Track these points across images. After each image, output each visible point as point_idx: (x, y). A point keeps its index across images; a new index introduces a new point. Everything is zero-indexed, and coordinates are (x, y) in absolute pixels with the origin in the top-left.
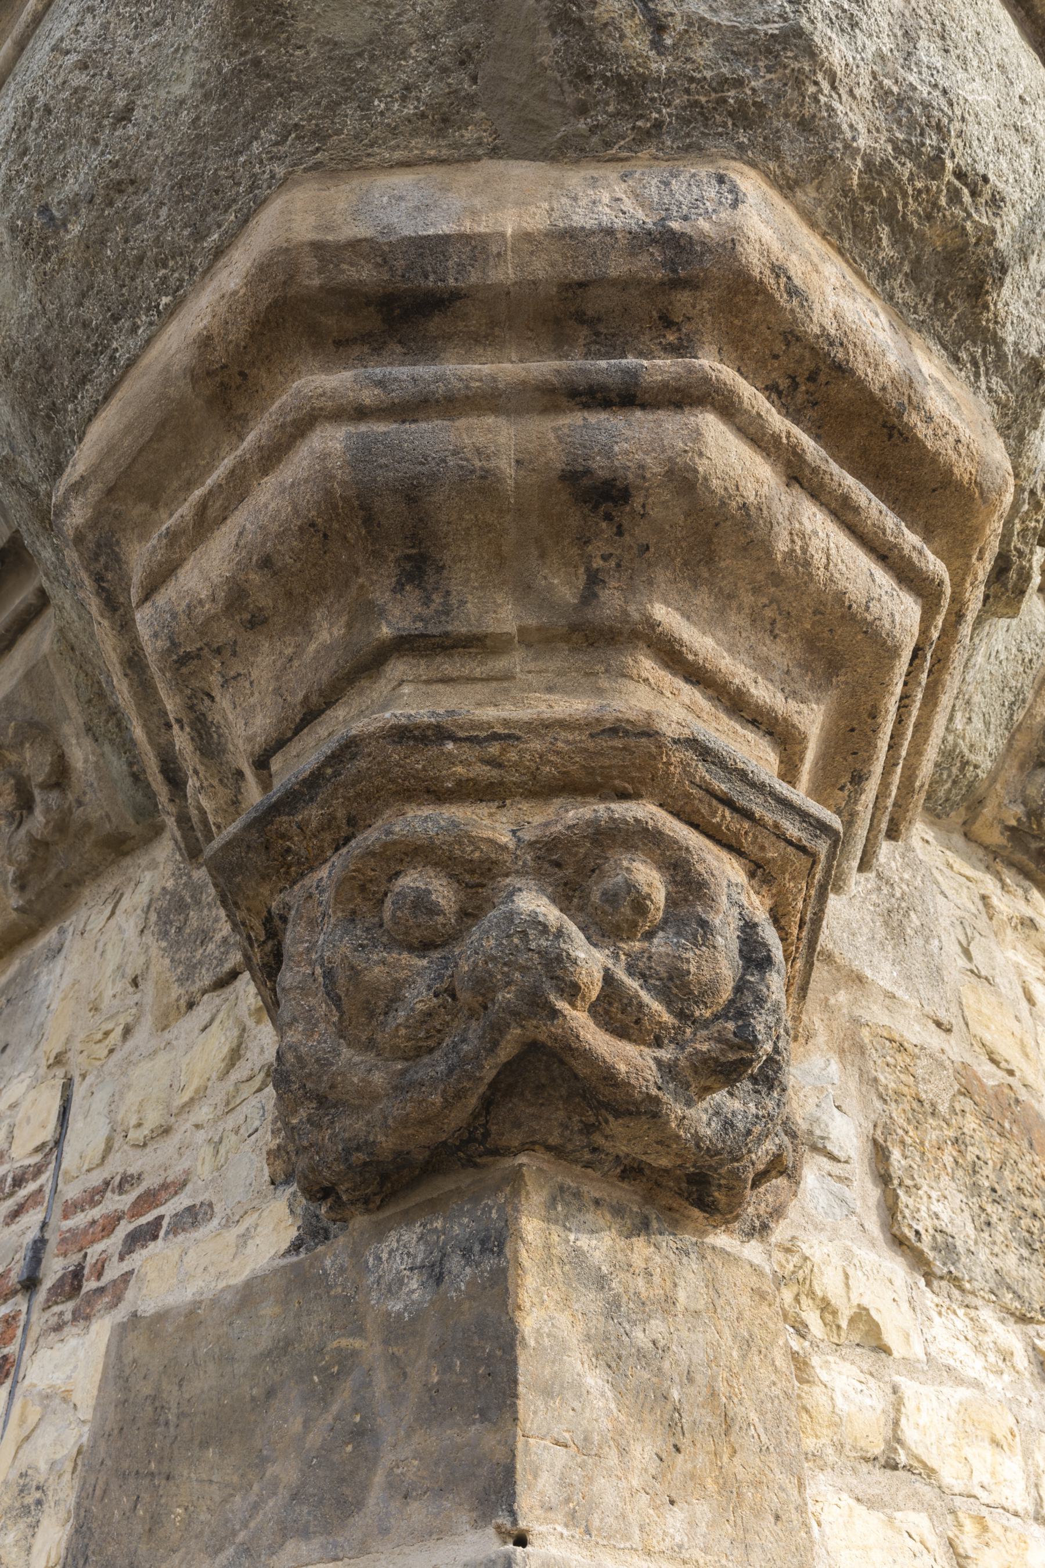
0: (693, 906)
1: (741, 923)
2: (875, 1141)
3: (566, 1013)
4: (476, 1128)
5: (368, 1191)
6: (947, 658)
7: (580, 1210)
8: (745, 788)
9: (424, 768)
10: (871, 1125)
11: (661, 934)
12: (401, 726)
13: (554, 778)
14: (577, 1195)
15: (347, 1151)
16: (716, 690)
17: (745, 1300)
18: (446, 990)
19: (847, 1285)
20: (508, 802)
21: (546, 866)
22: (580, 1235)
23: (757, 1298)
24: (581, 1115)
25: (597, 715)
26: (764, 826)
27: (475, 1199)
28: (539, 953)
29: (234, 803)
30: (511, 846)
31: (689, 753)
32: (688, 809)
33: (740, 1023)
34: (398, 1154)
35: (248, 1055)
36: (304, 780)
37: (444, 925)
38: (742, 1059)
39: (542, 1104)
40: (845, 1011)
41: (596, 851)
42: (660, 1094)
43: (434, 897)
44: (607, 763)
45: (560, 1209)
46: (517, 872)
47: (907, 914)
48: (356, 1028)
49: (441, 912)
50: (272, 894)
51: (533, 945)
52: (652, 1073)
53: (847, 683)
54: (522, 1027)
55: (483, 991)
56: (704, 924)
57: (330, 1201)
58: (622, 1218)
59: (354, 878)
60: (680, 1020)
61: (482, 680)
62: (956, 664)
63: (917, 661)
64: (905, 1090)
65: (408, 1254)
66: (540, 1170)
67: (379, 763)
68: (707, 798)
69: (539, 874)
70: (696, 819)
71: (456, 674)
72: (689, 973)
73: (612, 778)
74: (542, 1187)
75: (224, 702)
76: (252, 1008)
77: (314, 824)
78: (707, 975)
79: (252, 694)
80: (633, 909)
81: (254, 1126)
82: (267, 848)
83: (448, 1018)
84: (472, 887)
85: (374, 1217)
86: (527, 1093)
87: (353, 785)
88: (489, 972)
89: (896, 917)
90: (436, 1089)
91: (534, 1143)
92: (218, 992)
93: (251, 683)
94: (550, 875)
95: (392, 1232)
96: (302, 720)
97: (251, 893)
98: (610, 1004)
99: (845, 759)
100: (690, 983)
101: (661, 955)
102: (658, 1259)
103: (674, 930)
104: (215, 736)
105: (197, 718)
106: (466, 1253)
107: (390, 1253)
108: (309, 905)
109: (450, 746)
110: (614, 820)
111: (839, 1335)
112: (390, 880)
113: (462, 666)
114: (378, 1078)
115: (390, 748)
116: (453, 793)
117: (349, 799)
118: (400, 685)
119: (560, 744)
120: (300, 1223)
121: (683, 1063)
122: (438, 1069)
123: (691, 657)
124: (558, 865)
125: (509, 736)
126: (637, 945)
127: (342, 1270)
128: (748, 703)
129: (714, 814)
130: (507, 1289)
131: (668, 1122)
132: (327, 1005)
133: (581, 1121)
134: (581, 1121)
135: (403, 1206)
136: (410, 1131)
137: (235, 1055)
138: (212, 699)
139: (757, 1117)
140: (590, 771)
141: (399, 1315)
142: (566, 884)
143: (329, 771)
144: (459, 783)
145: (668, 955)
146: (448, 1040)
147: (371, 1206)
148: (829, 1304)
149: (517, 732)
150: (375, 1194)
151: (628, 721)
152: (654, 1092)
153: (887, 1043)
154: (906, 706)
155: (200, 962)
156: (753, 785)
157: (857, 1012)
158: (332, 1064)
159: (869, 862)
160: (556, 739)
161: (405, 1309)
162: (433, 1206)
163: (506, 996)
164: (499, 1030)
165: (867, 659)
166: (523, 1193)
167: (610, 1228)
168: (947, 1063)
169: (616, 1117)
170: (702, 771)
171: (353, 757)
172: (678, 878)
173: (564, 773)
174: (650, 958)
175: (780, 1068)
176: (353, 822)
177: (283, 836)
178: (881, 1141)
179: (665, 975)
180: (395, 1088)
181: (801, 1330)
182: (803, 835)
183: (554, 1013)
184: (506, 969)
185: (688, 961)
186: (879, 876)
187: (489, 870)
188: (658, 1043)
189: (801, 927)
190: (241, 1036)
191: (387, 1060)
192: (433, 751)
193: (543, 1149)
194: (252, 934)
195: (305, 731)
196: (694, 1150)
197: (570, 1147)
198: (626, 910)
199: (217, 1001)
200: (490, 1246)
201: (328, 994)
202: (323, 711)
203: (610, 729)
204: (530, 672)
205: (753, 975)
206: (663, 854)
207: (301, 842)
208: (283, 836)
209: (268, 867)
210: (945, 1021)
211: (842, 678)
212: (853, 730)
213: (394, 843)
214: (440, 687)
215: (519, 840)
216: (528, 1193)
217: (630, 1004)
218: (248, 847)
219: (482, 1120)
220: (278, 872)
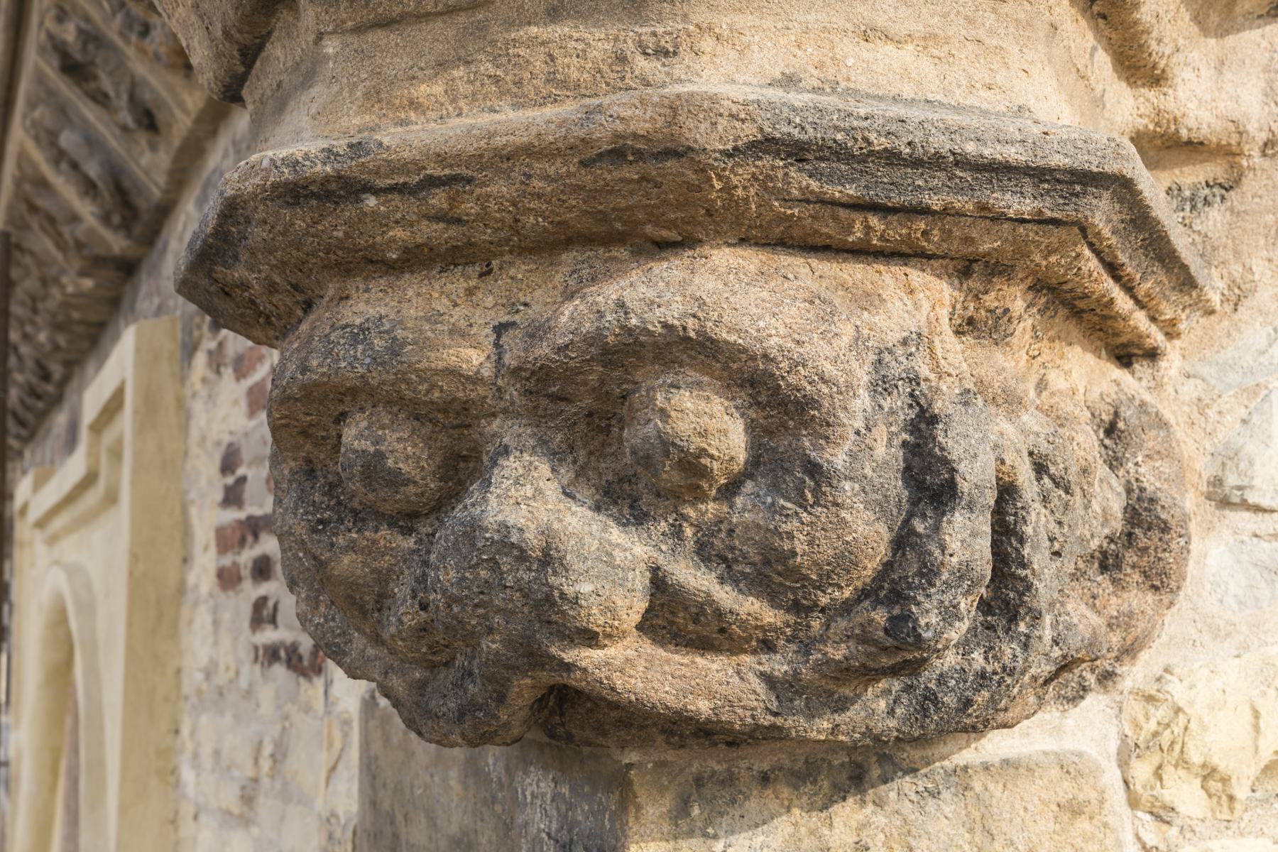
0: (797, 437)
1: (912, 414)
3: (584, 664)
7: (733, 801)
8: (897, 174)
12: (286, 184)
13: (545, 230)
14: (729, 780)
17: (1046, 825)
19: (1256, 728)
21: (544, 402)
22: (732, 839)
23: (1066, 817)
25: (582, 134)
26: (960, 214)
28: (521, 590)
30: (487, 372)
31: (767, 161)
32: (796, 232)
33: (896, 611)
38: (905, 661)
42: (779, 721)
44: (623, 203)
46: (505, 411)
49: (408, 482)
56: (813, 469)
58: (815, 782)
60: (798, 614)
66: (661, 765)
67: (283, 234)
68: (828, 210)
69: (536, 416)
70: (819, 241)
72: (794, 554)
74: (662, 790)
78: (827, 551)
80: (683, 469)
88: (455, 617)
94: (553, 417)
100: (800, 566)
101: (747, 528)
102: (880, 820)
109: (371, 201)
110: (629, 331)
111: (1232, 809)
115: (287, 213)
126: (711, 509)
129: (849, 229)
139: (983, 675)
140: (603, 217)
142: (590, 415)
144: (406, 250)
145: (758, 526)
148: (1214, 770)
151: (635, 136)
152: (767, 720)
156: (916, 163)
160: (529, 177)
163: (491, 645)
166: (632, 810)
167: (789, 810)
170: (800, 180)
173: (559, 223)
174: (731, 532)
175: (1029, 587)
179: (757, 558)
181: (1162, 814)
184: (481, 611)
185: (791, 536)
188: (767, 646)
192: (349, 211)
203: (610, 152)
205: (924, 517)
206: (726, 368)
214: (379, 36)
216: (639, 808)
217: (702, 611)
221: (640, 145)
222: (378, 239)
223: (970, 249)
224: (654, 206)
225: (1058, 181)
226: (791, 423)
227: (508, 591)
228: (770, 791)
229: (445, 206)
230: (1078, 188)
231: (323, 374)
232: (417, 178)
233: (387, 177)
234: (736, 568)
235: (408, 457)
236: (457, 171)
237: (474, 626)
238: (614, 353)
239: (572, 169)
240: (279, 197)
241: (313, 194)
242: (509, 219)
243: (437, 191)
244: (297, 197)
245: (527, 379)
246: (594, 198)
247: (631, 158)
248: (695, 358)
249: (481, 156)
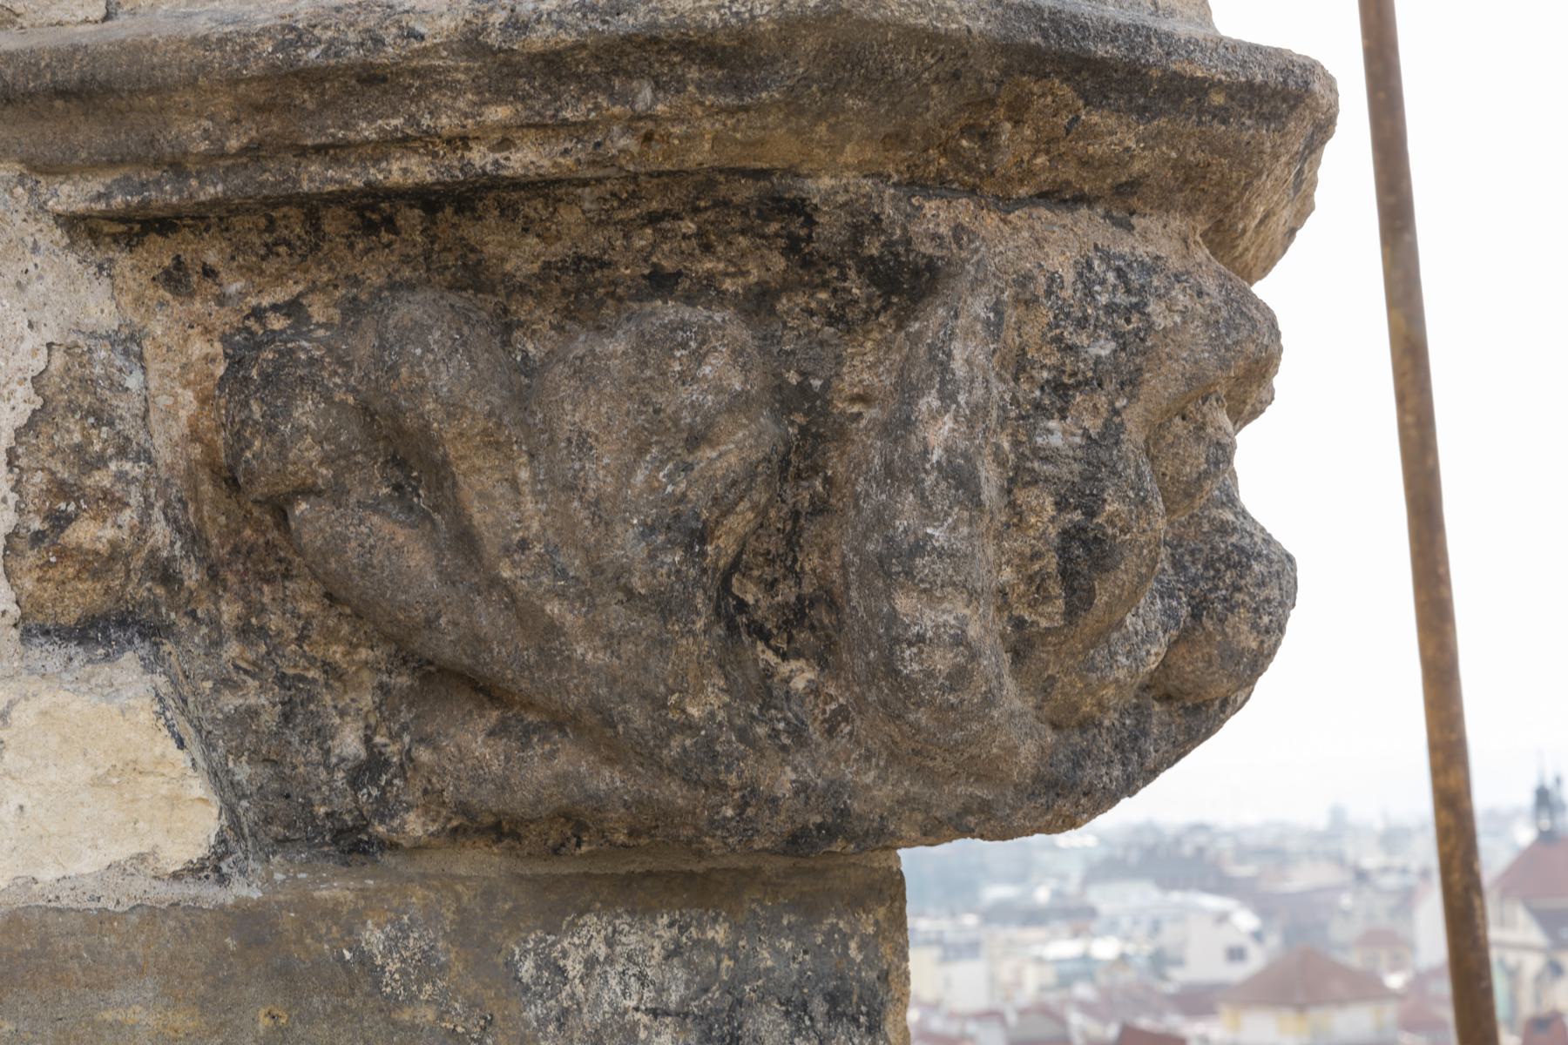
65: (642, 978)
95: (590, 919)
106: (796, 1010)
107: (590, 962)
127: (427, 967)
132: (1037, 583)
200: (850, 1011)
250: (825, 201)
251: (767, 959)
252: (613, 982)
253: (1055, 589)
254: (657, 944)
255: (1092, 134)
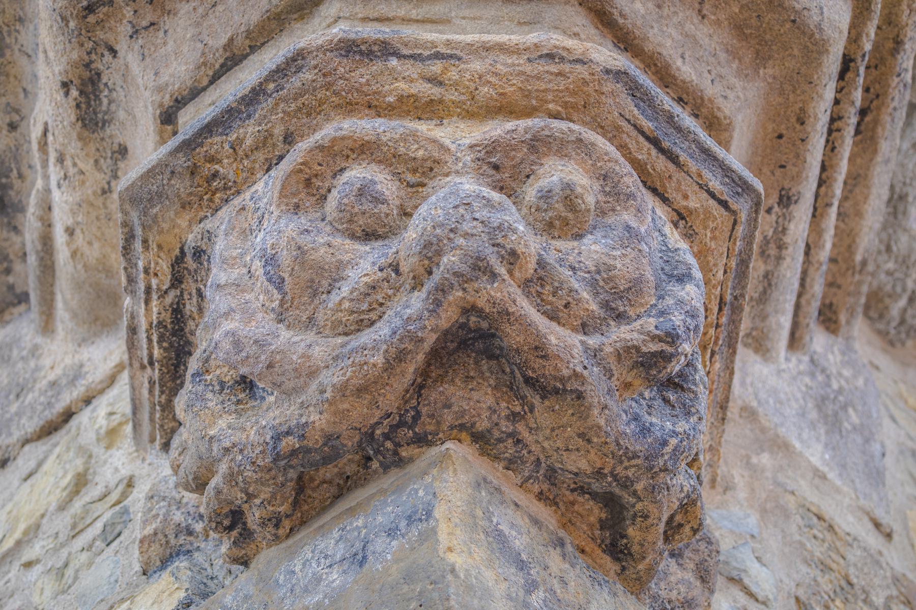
2: (797, 599)
4: (407, 411)
5: (281, 509)
6: (886, 93)
9: (368, 83)
10: (793, 584)
11: (590, 236)
13: (491, 98)
15: (277, 438)
16: (642, 61)
18: (390, 265)
20: (444, 121)
21: (485, 167)
24: (508, 403)
25: (536, 41)
27: (399, 490)
28: (482, 222)
29: (104, 192)
34: (329, 438)
35: (97, 479)
36: (243, 98)
37: (387, 215)
39: (472, 390)
40: (769, 474)
41: (532, 157)
42: (585, 373)
43: (379, 187)
44: (544, 87)
45: (483, 494)
46: (457, 172)
47: (844, 408)
48: (297, 308)
50: (190, 225)
51: (477, 215)
52: (578, 350)
53: (774, 78)
54: (464, 290)
55: (430, 254)
57: (235, 533)
59: (300, 171)
61: (417, 21)
62: (895, 103)
63: (849, 75)
64: (834, 566)
65: (326, 557)
68: (634, 133)
71: (391, 15)
73: (546, 102)
75: (129, 55)
76: (103, 431)
77: (249, 142)
79: (165, 44)
81: (116, 532)
82: (192, 173)
83: (390, 292)
84: (412, 186)
85: (283, 545)
86: (457, 380)
87: (295, 99)
89: (830, 408)
90: (378, 350)
91: (462, 427)
92: (45, 440)
93: (166, 32)
96: (222, 66)
97: (165, 226)
98: (542, 286)
99: (773, 173)
100: (615, 276)
103: (603, 234)
104: (105, 101)
105: (91, 80)
106: (392, 532)
107: (304, 565)
108: (241, 218)
109: (394, 62)
112: (334, 176)
113: (398, 7)
114: (318, 352)
115: (337, 60)
116: (394, 108)
117: (289, 114)
118: (336, 21)
119: (499, 66)
120: (187, 585)
121: (608, 349)
122: (380, 333)
123: (621, 21)
124: (496, 167)
125: (451, 56)
128: (674, 77)
130: (438, 540)
131: (590, 408)
132: (267, 292)
133: (508, 408)
134: (508, 408)
135: (316, 525)
136: (346, 406)
137: (81, 482)
138: (113, 52)
140: (527, 95)
141: (319, 605)
143: (271, 86)
144: (401, 99)
146: (389, 312)
147: (281, 532)
149: (458, 52)
150: (287, 516)
151: (564, 48)
152: (579, 369)
153: (815, 520)
154: (839, 130)
155: (19, 414)
157: (781, 478)
158: (270, 344)
159: (801, 338)
161: (325, 597)
162: (351, 512)
164: (443, 290)
165: (796, 52)
168: (884, 565)
169: (543, 398)
171: (299, 69)
172: (607, 189)
173: (502, 94)
176: (289, 139)
177: (212, 160)
178: (803, 598)
179: (593, 269)
180: (336, 358)
182: (725, 189)
183: (494, 276)
184: (452, 235)
186: (812, 361)
187: (431, 169)
188: (584, 328)
189: (720, 310)
190: (87, 463)
191: (327, 337)
192: (377, 66)
193: (468, 439)
194: (154, 282)
195: (223, 78)
196: (613, 447)
197: (496, 434)
198: (560, 206)
199: (44, 448)
200: (418, 516)
201: (270, 280)
202: (245, 57)
203: (547, 55)
204: (464, 18)
207: (231, 164)
208: (212, 160)
209: (191, 194)
210: (885, 519)
211: (770, 71)
212: (780, 137)
213: (343, 138)
215: (459, 145)
216: (455, 470)
218: (173, 172)
219: (414, 402)
220: (201, 199)
221: (565, 54)
222: (387, 87)
223: (685, 203)
224: (561, 91)
225: (734, 181)
226: (618, 208)
227: (475, 223)
228: (518, 512)
229: (439, 72)
230: (740, 190)
231: (351, 132)
232: (429, 53)
233: (411, 48)
234: (578, 273)
235: (388, 189)
236: (455, 52)
237: (444, 245)
238: (537, 141)
239: (522, 62)
240: (337, 50)
241: (361, 53)
242: (472, 86)
243: (438, 62)
244: (349, 51)
245: (480, 151)
246: (528, 81)
247: (557, 61)
248: (579, 155)
249: (472, 45)
250: (196, 242)
251: (380, 519)
252: (313, 565)
253: (270, 288)
254: (333, 541)
255: (240, 141)
